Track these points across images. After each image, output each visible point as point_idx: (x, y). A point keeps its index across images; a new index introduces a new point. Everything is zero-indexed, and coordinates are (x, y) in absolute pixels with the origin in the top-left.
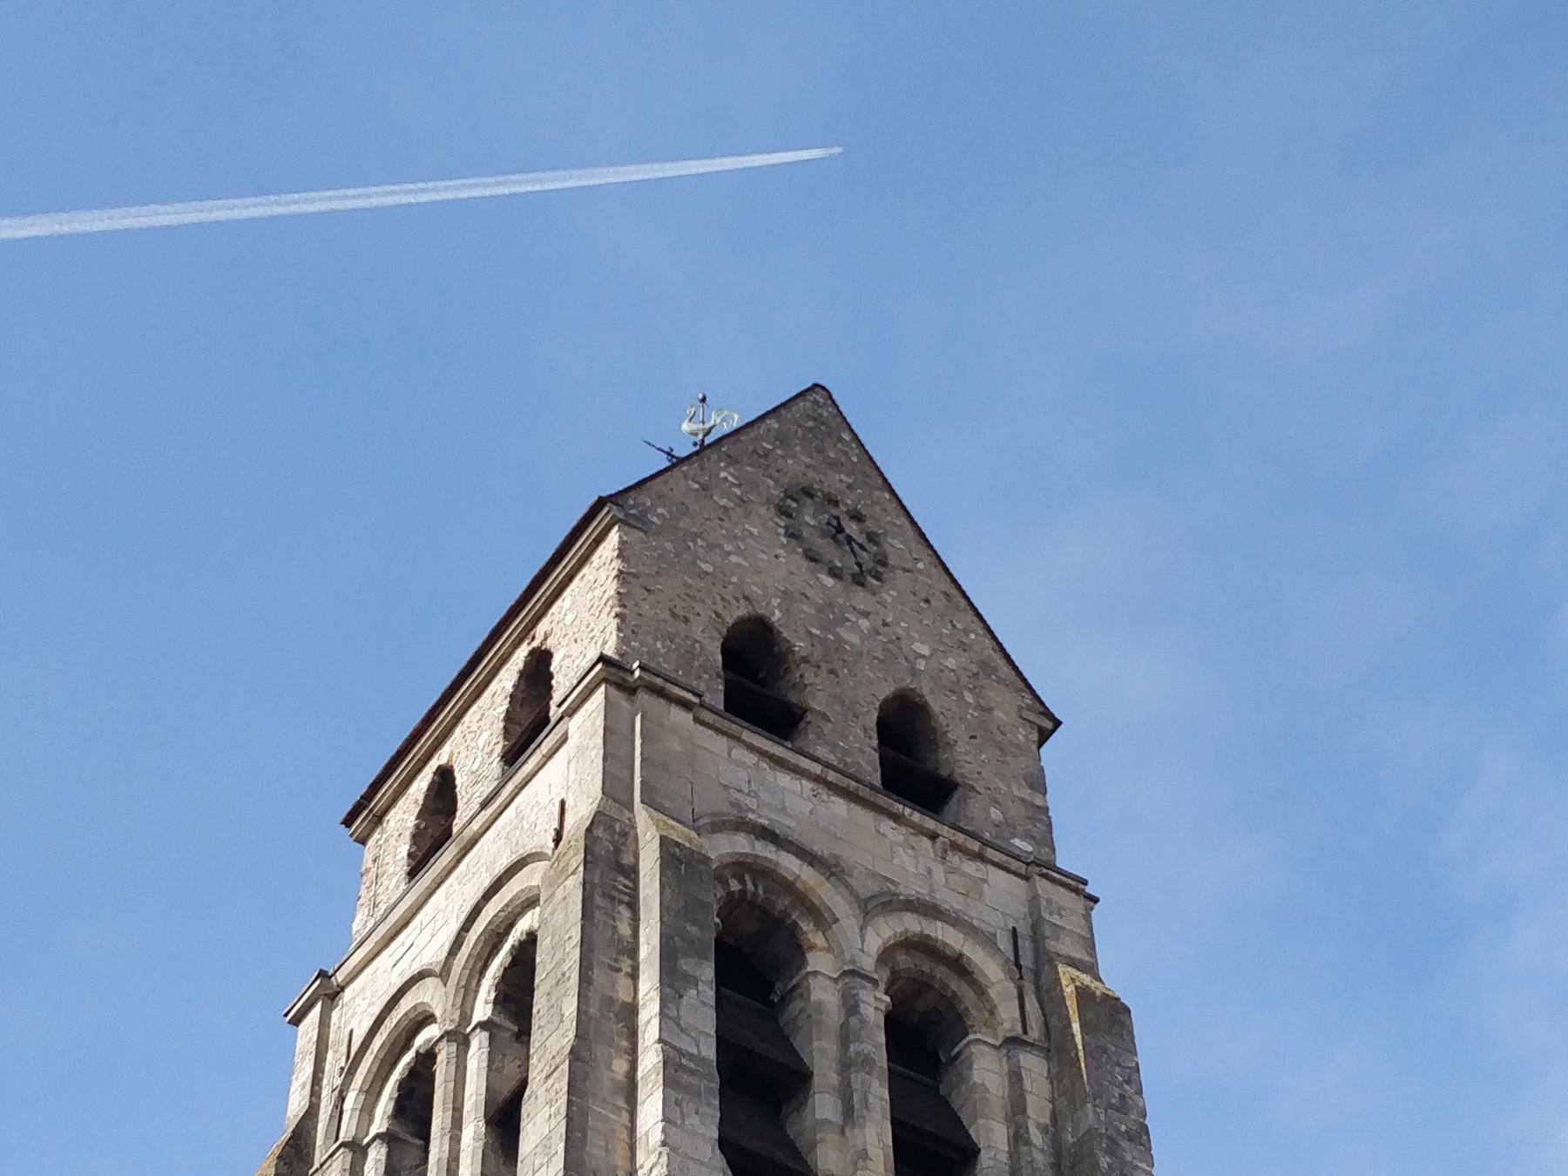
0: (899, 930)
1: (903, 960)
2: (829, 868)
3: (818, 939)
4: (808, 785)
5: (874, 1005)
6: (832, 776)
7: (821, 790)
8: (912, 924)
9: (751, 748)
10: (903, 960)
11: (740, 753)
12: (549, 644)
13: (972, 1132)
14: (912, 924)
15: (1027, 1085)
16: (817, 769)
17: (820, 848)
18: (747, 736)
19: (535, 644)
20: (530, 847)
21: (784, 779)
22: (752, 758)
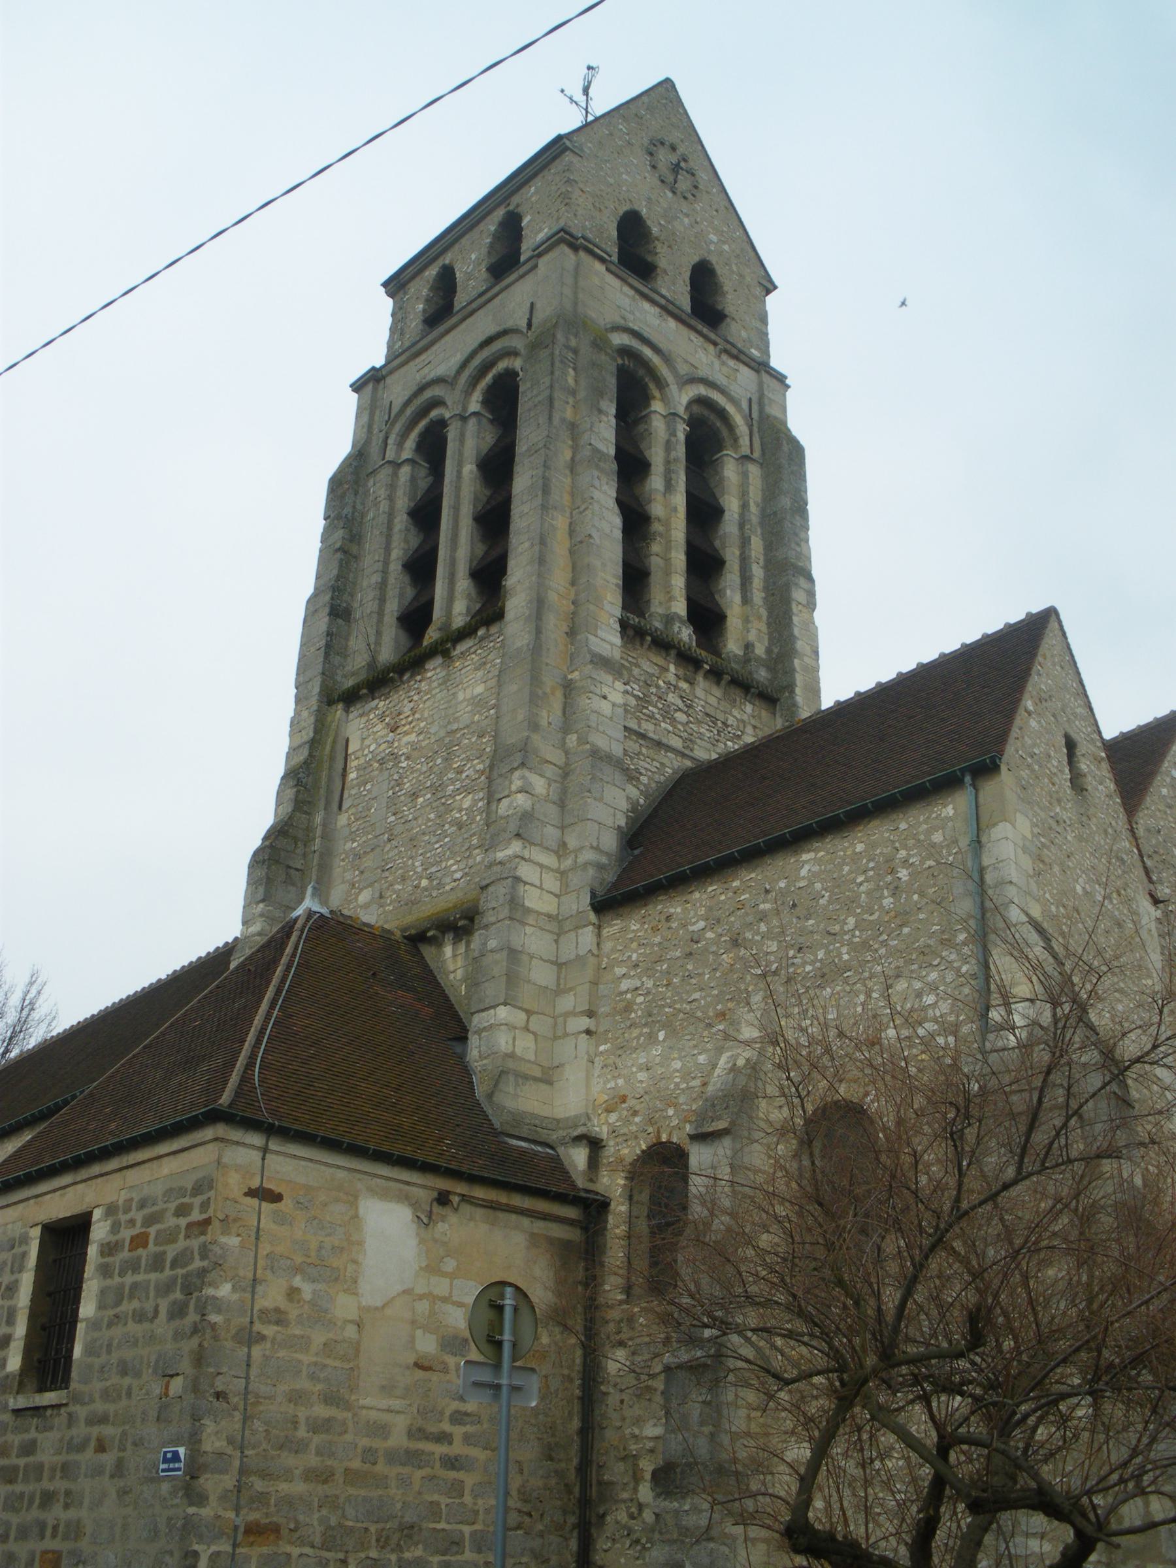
0: (697, 392)
1: (696, 409)
2: (667, 358)
3: (656, 393)
4: (658, 310)
5: (682, 430)
6: (671, 307)
7: (664, 313)
8: (702, 390)
9: (631, 287)
10: (696, 409)
11: (626, 289)
12: (520, 210)
13: (721, 501)
14: (702, 390)
15: (751, 480)
16: (663, 302)
17: (663, 345)
18: (631, 280)
19: (511, 208)
20: (509, 324)
21: (646, 305)
22: (631, 292)
